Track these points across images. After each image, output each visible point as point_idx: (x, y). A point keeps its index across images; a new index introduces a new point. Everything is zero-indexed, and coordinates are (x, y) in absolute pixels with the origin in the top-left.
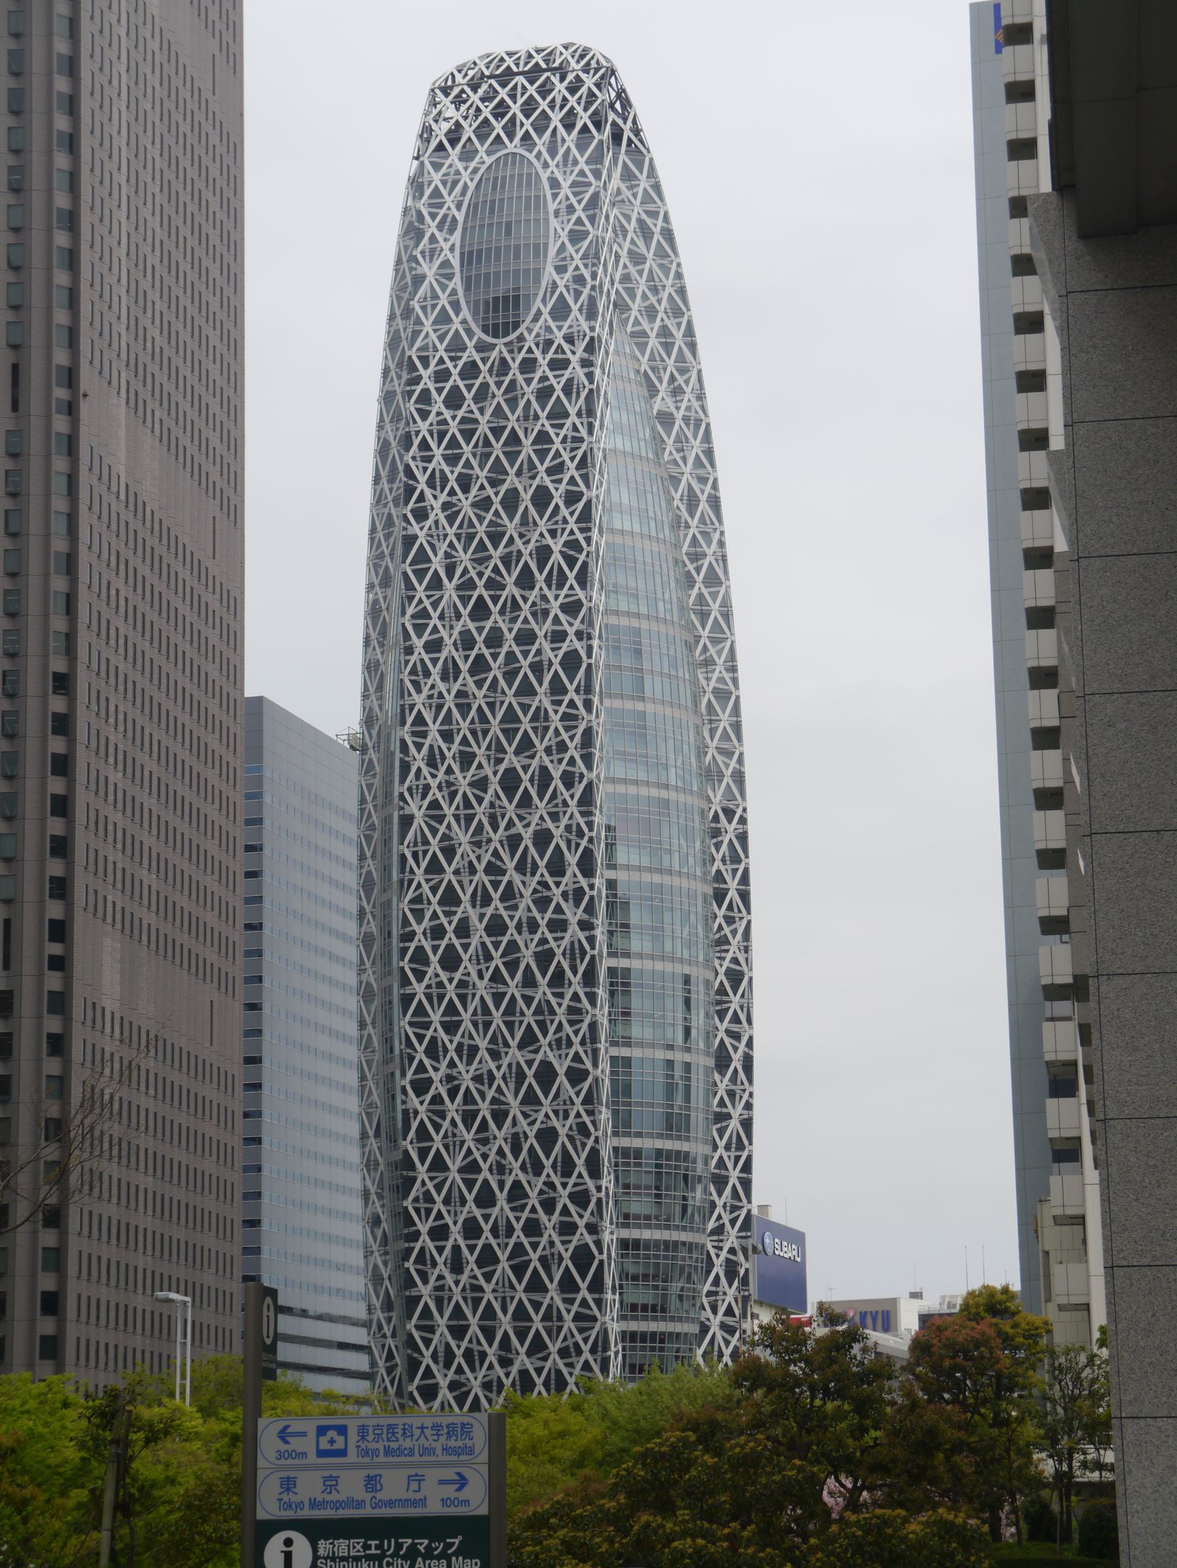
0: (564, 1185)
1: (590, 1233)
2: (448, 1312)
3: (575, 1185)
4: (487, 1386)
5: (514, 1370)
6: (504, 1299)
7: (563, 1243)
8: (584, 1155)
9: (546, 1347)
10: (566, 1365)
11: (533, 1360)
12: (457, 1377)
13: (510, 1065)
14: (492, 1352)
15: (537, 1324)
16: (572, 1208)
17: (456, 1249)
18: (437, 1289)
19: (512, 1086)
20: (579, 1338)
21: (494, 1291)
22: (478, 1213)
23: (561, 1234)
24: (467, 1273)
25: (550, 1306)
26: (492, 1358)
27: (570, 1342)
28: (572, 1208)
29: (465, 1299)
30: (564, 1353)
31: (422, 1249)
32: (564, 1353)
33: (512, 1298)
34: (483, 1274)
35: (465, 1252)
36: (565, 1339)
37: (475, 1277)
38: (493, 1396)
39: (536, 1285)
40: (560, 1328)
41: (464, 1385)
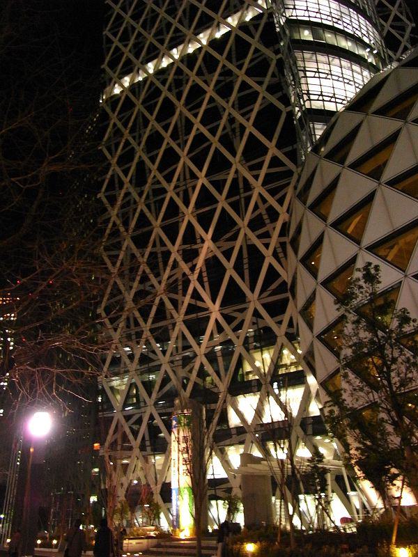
0: (240, 67)
1: (272, 93)
2: (133, 224)
3: (252, 61)
4: (172, 288)
5: (200, 262)
6: (186, 192)
7: (243, 115)
8: (257, 36)
9: (235, 224)
10: (259, 237)
11: (220, 243)
12: (142, 287)
13: (184, 11)
14: (175, 250)
15: (222, 203)
16: (250, 81)
17: (141, 164)
18: (123, 207)
19: (186, 22)
20: (272, 201)
21: (176, 187)
22: (159, 128)
23: (240, 109)
24: (150, 180)
25: (235, 181)
26: (175, 255)
27: (262, 209)
28: (250, 81)
29: (148, 206)
30: (255, 224)
31: (112, 176)
32: (255, 224)
33: (194, 188)
34: (165, 177)
35: (148, 162)
36: (256, 207)
37: (159, 182)
38: (178, 297)
39: (220, 164)
40: (248, 199)
41: (148, 293)
